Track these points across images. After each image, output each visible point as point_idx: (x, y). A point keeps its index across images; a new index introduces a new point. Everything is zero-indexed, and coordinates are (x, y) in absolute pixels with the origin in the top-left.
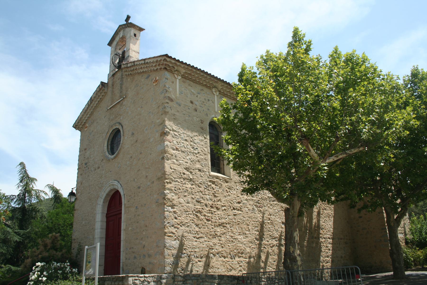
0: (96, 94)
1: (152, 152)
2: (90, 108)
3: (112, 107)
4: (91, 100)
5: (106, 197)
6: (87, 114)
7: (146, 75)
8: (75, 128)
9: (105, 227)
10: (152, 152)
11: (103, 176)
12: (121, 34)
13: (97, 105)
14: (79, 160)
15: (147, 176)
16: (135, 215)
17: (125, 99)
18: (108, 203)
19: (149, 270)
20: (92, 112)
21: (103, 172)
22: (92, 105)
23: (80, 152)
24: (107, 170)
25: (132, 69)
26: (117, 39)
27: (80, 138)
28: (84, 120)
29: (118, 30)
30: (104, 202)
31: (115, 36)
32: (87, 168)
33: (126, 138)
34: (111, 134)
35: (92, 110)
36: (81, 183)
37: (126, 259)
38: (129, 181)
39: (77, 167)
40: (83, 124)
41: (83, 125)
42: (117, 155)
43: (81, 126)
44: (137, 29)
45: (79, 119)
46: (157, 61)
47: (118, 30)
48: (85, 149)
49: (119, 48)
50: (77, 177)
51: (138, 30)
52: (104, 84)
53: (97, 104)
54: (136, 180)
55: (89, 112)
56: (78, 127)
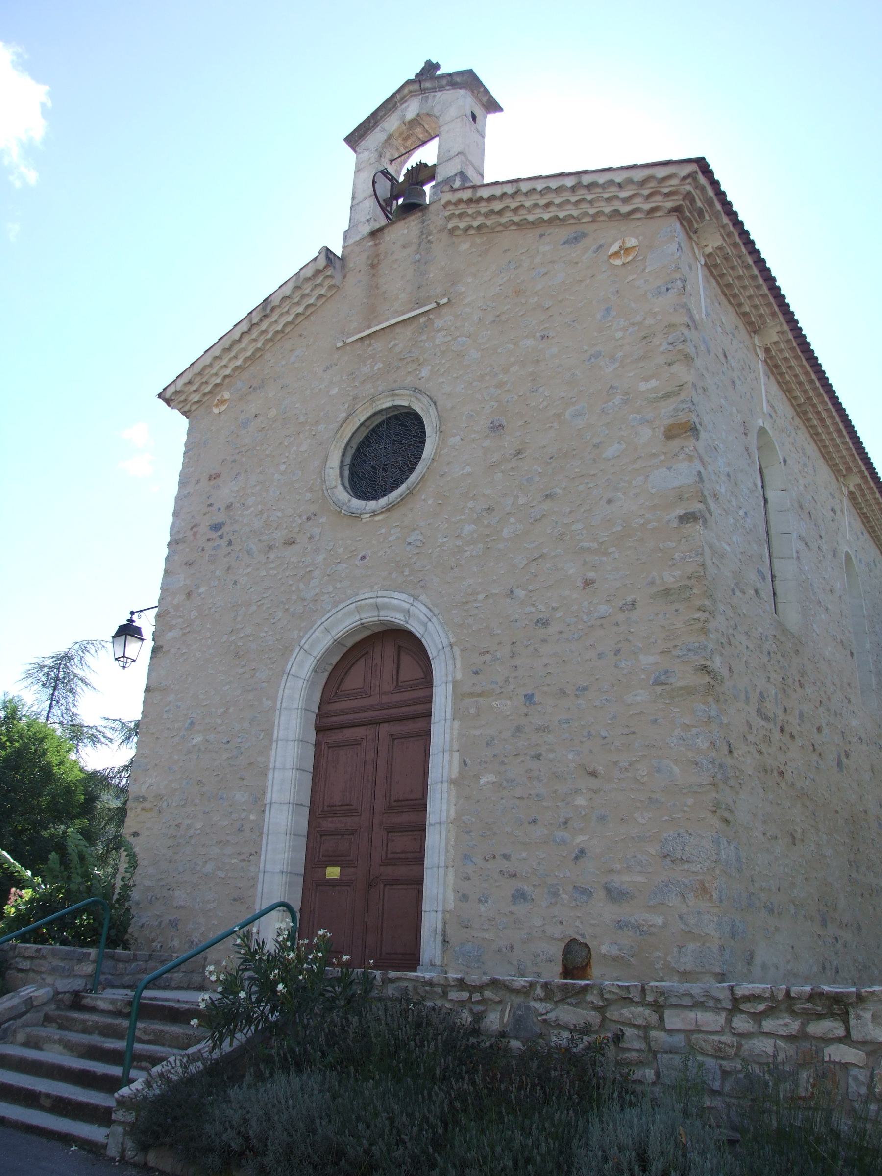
0: (297, 288)
1: (620, 495)
2: (255, 334)
3: (369, 335)
4: (267, 307)
5: (329, 652)
6: (236, 357)
7: (564, 233)
8: (168, 402)
9: (309, 765)
10: (620, 495)
11: (317, 573)
12: (412, 109)
13: (288, 330)
14: (176, 514)
15: (588, 583)
16: (519, 729)
17: (445, 311)
18: (326, 674)
19: (615, 951)
20: (258, 350)
21: (320, 558)
22: (263, 327)
23: (183, 483)
24: (341, 550)
25: (497, 206)
26: (392, 124)
27: (184, 438)
28: (216, 374)
29: (398, 96)
30: (315, 671)
31: (381, 114)
32: (223, 543)
33: (454, 440)
34: (362, 424)
35: (259, 345)
36: (189, 595)
37: (465, 898)
38: (481, 597)
39: (168, 538)
40: (208, 388)
41: (205, 395)
42: (403, 499)
43: (196, 397)
44: (480, 101)
45: (198, 368)
46: (643, 183)
47: (398, 96)
48: (216, 477)
49: (388, 156)
50: (166, 572)
51: (483, 105)
52: (331, 256)
53: (286, 325)
54: (521, 593)
55: (244, 350)
56: (182, 399)
